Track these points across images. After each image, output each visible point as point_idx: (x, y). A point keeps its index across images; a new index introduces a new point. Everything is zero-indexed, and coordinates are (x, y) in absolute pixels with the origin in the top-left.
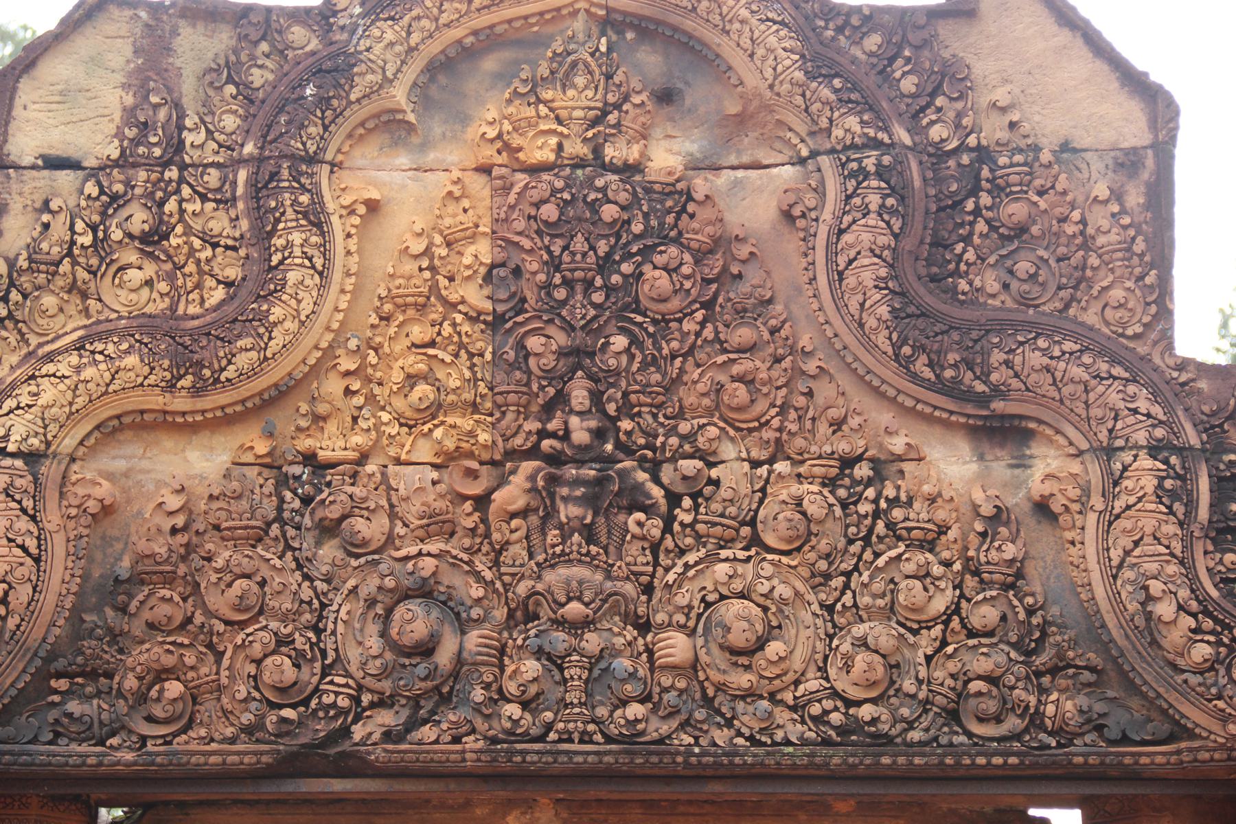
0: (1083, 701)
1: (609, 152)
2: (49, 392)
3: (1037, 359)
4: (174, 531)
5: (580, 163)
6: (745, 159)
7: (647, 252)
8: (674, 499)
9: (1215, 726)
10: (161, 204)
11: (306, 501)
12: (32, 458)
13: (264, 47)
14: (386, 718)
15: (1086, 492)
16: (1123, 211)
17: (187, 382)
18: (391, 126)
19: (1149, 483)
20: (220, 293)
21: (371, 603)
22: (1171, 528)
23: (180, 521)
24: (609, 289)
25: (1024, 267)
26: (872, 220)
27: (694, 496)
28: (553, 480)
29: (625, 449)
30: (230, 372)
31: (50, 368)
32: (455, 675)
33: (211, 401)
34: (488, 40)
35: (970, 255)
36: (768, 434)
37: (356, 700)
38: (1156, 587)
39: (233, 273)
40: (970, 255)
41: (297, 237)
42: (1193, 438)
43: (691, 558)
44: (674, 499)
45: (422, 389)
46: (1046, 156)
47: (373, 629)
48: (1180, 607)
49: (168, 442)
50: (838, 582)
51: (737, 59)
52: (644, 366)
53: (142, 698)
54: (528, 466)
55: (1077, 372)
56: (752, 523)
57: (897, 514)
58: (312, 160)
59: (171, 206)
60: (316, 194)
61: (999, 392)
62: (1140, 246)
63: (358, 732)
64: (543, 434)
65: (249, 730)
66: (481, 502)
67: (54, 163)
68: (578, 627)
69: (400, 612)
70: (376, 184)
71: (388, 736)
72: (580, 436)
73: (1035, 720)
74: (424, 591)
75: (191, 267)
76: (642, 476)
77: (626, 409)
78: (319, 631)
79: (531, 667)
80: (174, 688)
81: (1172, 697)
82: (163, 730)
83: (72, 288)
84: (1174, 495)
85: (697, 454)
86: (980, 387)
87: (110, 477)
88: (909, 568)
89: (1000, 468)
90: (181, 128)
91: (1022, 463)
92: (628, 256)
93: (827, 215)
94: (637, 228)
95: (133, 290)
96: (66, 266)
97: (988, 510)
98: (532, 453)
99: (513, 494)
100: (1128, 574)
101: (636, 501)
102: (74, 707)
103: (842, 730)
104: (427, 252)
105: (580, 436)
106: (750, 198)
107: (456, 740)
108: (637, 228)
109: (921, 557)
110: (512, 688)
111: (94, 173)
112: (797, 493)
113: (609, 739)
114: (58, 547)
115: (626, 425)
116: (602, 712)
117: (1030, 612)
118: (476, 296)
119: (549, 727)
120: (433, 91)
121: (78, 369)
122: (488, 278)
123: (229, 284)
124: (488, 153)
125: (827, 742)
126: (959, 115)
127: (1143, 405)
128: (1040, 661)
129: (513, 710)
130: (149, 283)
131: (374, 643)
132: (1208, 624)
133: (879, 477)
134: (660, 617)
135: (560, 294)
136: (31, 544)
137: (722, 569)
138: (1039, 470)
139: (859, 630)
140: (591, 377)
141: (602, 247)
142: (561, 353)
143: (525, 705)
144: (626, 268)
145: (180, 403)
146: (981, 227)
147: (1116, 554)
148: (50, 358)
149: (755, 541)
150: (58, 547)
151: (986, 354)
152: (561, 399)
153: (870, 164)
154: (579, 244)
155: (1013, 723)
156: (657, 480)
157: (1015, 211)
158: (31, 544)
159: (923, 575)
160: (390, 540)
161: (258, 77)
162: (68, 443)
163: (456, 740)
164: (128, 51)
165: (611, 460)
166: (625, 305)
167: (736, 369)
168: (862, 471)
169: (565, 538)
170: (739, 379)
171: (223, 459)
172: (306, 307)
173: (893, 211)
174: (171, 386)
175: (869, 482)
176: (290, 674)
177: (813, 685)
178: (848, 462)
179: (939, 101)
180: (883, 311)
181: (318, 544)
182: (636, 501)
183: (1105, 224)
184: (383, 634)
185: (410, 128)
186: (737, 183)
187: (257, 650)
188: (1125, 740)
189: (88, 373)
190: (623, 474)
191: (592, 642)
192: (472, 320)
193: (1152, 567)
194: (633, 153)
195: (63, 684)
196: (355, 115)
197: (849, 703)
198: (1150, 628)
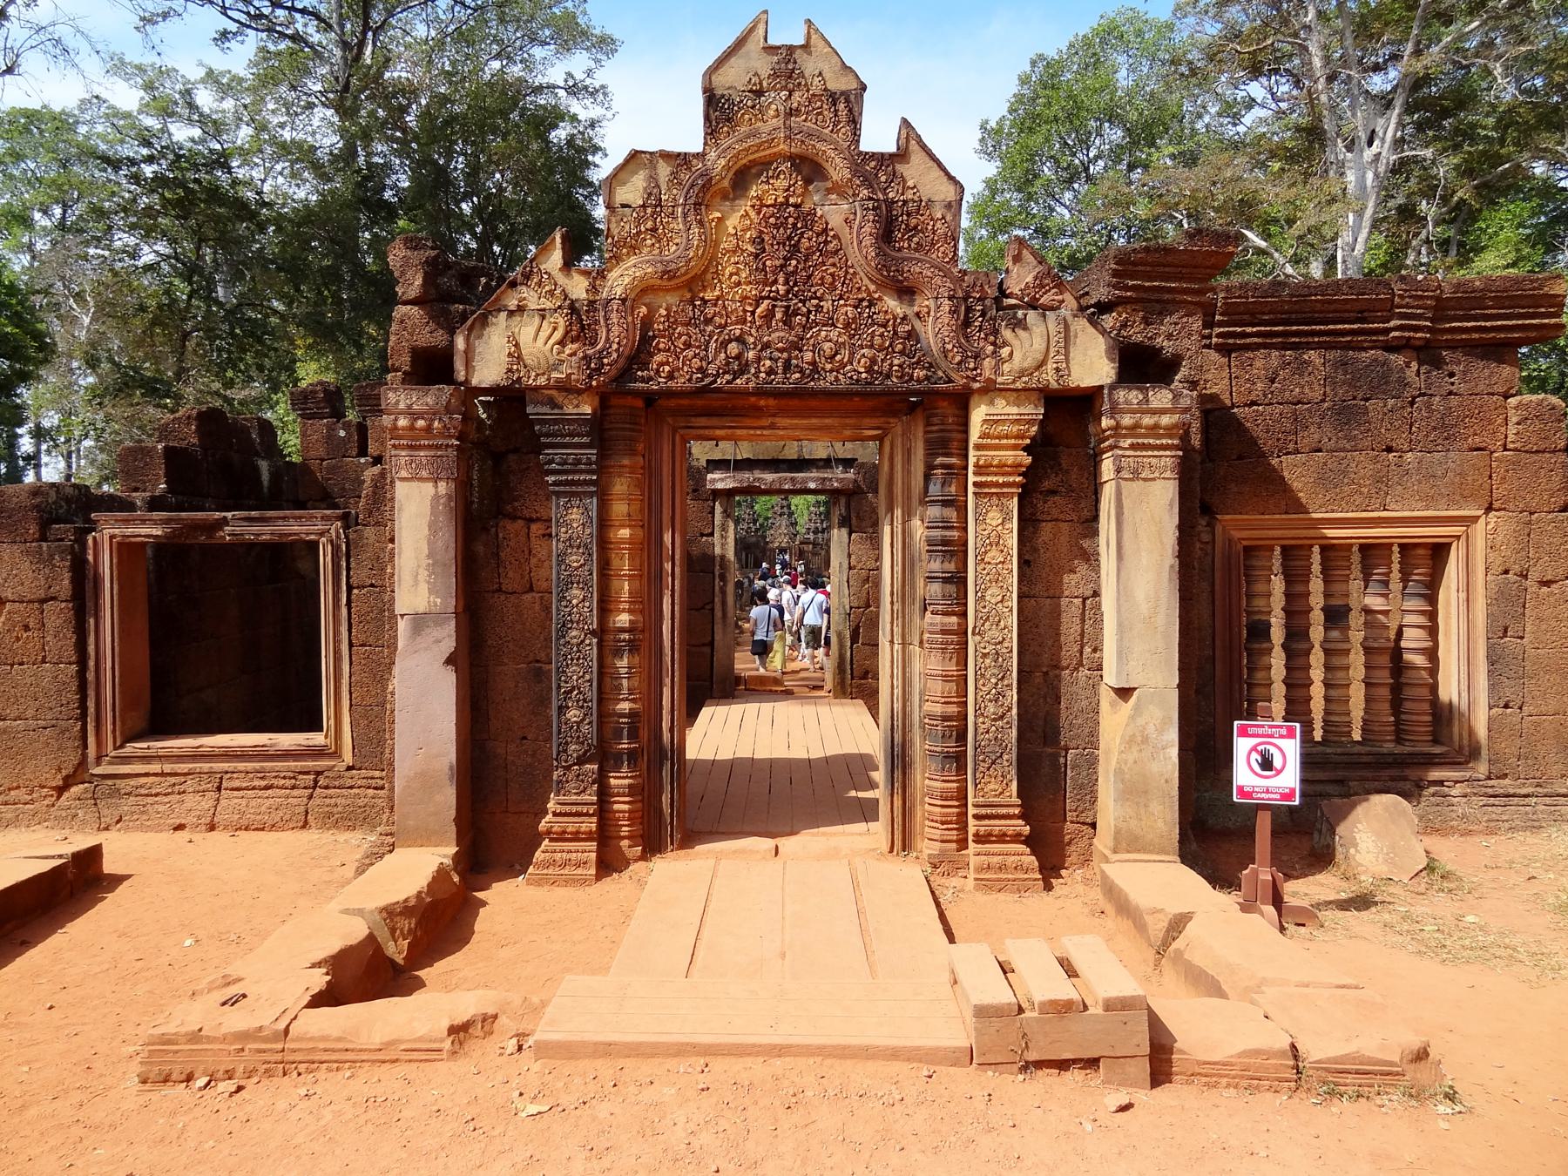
1: (792, 200)
5: (782, 204)
12: (624, 301)
14: (727, 377)
34: (754, 163)
44: (809, 312)
51: (831, 170)
65: (690, 380)
66: (753, 313)
67: (624, 206)
77: (795, 284)
79: (768, 363)
80: (667, 368)
98: (768, 298)
106: (834, 213)
129: (763, 375)
133: (871, 304)
157: (913, 222)
159: (882, 335)
178: (862, 300)
191: (785, 355)
198: (945, 352)
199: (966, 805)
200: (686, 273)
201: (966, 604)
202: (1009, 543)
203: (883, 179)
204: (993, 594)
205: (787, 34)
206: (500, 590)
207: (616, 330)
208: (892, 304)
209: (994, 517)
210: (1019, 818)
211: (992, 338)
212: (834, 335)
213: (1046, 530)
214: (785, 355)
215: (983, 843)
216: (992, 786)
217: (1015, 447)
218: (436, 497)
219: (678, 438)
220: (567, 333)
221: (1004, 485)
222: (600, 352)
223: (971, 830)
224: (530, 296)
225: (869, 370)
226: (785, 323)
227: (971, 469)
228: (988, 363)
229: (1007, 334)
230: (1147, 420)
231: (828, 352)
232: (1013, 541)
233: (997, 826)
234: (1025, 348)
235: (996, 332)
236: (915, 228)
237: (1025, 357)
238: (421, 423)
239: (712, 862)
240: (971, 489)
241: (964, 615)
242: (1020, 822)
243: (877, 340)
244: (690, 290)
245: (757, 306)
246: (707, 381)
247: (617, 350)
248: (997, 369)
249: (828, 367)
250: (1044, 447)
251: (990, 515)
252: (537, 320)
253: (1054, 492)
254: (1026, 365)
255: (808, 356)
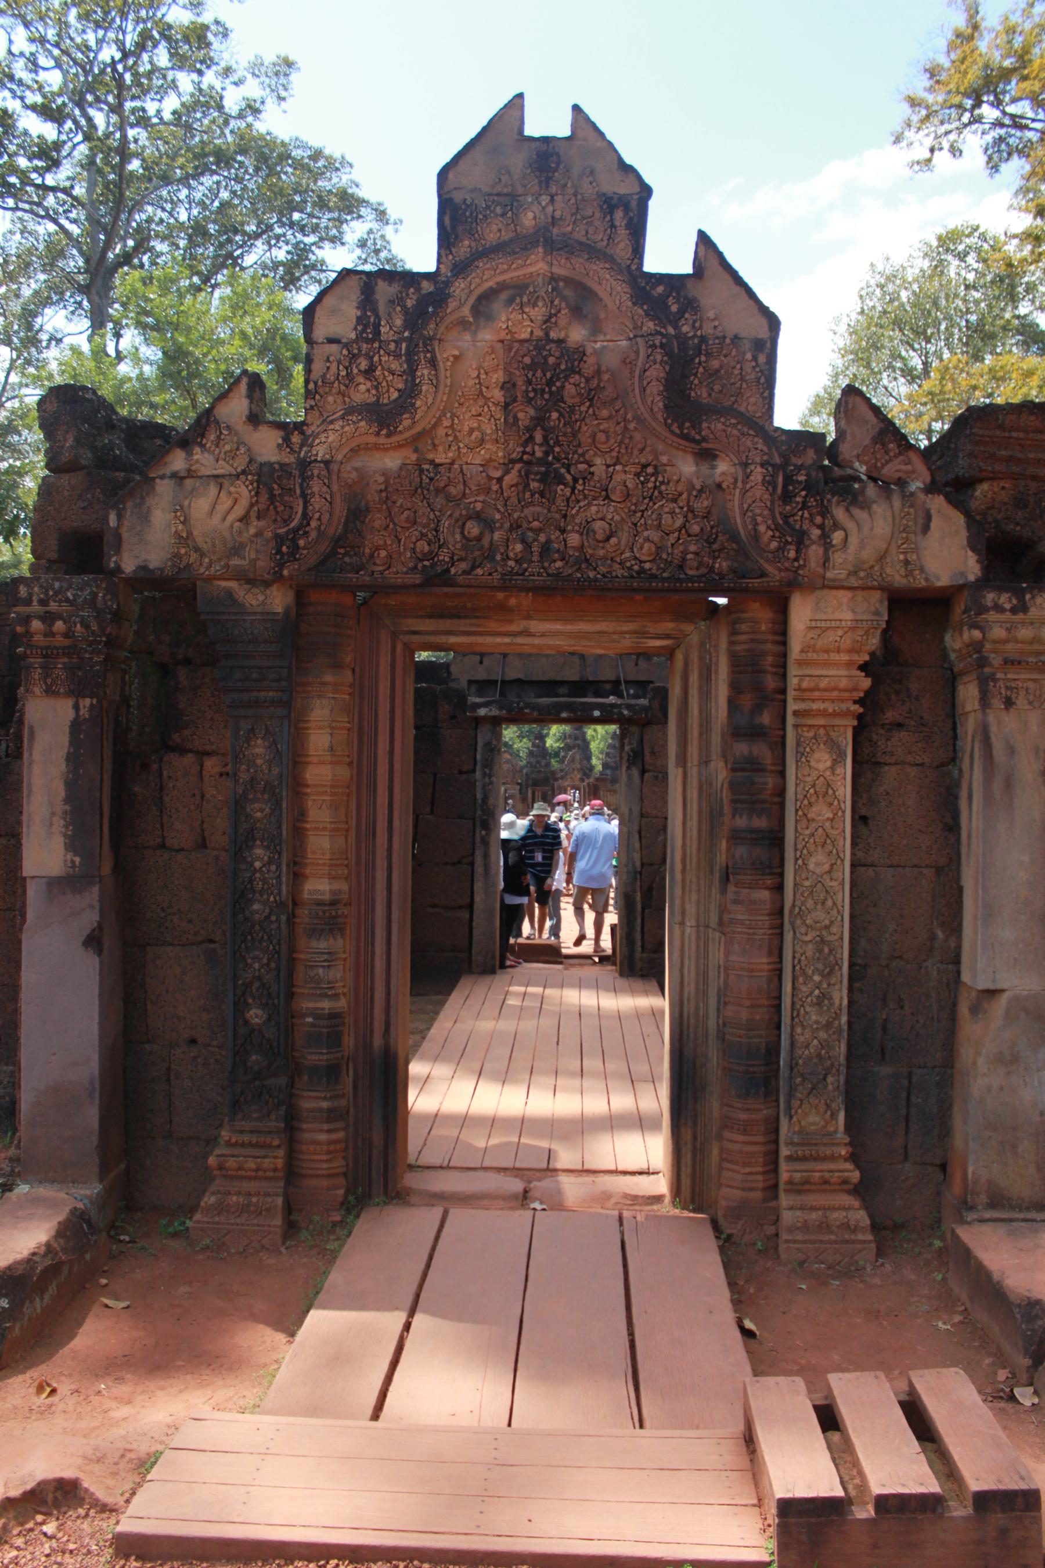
0: (729, 563)
2: (332, 437)
3: (720, 426)
4: (381, 491)
6: (608, 337)
7: (566, 378)
8: (575, 480)
9: (776, 573)
10: (372, 358)
11: (431, 479)
12: (327, 463)
13: (412, 290)
14: (464, 566)
15: (736, 480)
16: (757, 365)
17: (384, 432)
18: (463, 324)
19: (760, 478)
20: (396, 395)
21: (457, 520)
22: (767, 496)
23: (383, 487)
24: (551, 393)
25: (717, 388)
26: (657, 366)
27: (584, 479)
28: (527, 473)
29: (557, 459)
30: (401, 428)
31: (332, 427)
32: (490, 549)
33: (394, 439)
34: (502, 287)
35: (696, 382)
36: (614, 454)
37: (452, 558)
38: (759, 519)
39: (401, 386)
40: (696, 382)
41: (426, 372)
42: (777, 460)
43: (582, 504)
44: (575, 480)
45: (476, 434)
46: (728, 341)
47: (458, 530)
48: (768, 527)
49: (377, 455)
50: (639, 514)
52: (565, 425)
53: (372, 556)
54: (518, 466)
55: (735, 432)
56: (606, 490)
57: (663, 488)
58: (431, 339)
59: (376, 359)
60: (433, 352)
61: (704, 439)
62: (762, 380)
63: (453, 571)
64: (524, 453)
66: (500, 480)
67: (331, 341)
68: (537, 531)
69: (469, 524)
70: (458, 348)
71: (464, 572)
72: (539, 454)
73: (711, 569)
74: (478, 516)
75: (384, 384)
76: (563, 471)
77: (557, 443)
78: (437, 531)
79: (519, 547)
81: (762, 562)
82: (381, 568)
83: (339, 393)
84: (769, 483)
85: (586, 462)
86: (697, 437)
87: (356, 469)
88: (666, 510)
89: (705, 469)
90: (379, 325)
91: (713, 467)
92: (559, 379)
93: (639, 363)
94: (563, 367)
95: (362, 393)
96: (336, 384)
97: (698, 487)
98: (520, 460)
99: (511, 479)
100: (750, 514)
101: (560, 480)
102: (347, 560)
103: (638, 573)
104: (478, 377)
105: (539, 454)
107: (490, 574)
108: (563, 367)
109: (672, 505)
110: (511, 555)
111: (346, 346)
112: (624, 477)
113: (549, 575)
114: (338, 498)
115: (557, 449)
116: (546, 564)
117: (712, 527)
118: (498, 395)
119: (526, 570)
120: (481, 308)
121: (343, 427)
122: (502, 388)
123: (399, 391)
124: (503, 335)
125: (632, 577)
126: (694, 322)
127: (760, 446)
128: (715, 546)
129: (511, 563)
130: (368, 390)
131: (458, 537)
132: (777, 534)
134: (569, 528)
135: (531, 395)
136: (328, 497)
137: (594, 509)
138: (719, 471)
139: (646, 534)
140: (543, 429)
141: (548, 375)
142: (532, 419)
143: (516, 561)
144: (558, 384)
145: (382, 440)
146: (701, 370)
147: (745, 506)
148: (332, 422)
149: (607, 497)
150: (338, 498)
151: (700, 423)
152: (531, 439)
153: (657, 342)
154: (539, 374)
155: (703, 570)
156: (569, 472)
157: (715, 364)
158: (328, 497)
159: (672, 513)
160: (464, 494)
161: (409, 303)
162: (339, 457)
163: (490, 574)
164: (358, 293)
165: (551, 464)
166: (557, 398)
167: (601, 427)
168: (650, 470)
169: (532, 495)
170: (603, 431)
171: (399, 462)
172: (430, 401)
173: (666, 363)
174: (378, 434)
175: (653, 475)
176: (427, 548)
177: (627, 555)
178: (645, 466)
179: (687, 315)
180: (661, 404)
181: (437, 496)
182: (560, 480)
183: (749, 370)
184: (462, 533)
185: (471, 323)
186: (604, 347)
187: (414, 539)
188: (744, 577)
189: (347, 429)
190: (556, 470)
192: (496, 405)
193: (758, 511)
194: (562, 335)
195: (342, 551)
196: (448, 320)
197: (641, 562)
198: (756, 536)
199: (776, 1142)
200: (409, 428)
201: (781, 875)
202: (840, 793)
203: (674, 308)
204: (818, 862)
205: (548, 120)
206: (163, 846)
207: (317, 503)
208: (687, 467)
209: (822, 760)
210: (846, 1160)
211: (818, 520)
212: (609, 512)
213: (890, 775)
214: (542, 538)
215: (799, 1192)
216: (812, 1118)
217: (849, 665)
218: (75, 726)
219: (399, 647)
220: (252, 505)
221: (834, 715)
222: (295, 531)
223: (784, 1176)
224: (204, 461)
225: (656, 558)
226: (542, 494)
227: (791, 694)
228: (814, 552)
229: (839, 513)
230: (1025, 633)
231: (600, 536)
232: (845, 791)
233: (818, 1170)
234: (866, 533)
235: (825, 512)
236: (718, 371)
237: (862, 545)
238: (59, 625)
239: (437, 1213)
240: (790, 720)
241: (779, 888)
242: (849, 1166)
243: (666, 519)
244: (416, 450)
245: (507, 472)
246: (439, 569)
247: (318, 528)
248: (826, 560)
249: (602, 553)
250: (884, 667)
251: (817, 755)
252: (213, 490)
253: (900, 726)
254: (865, 554)
255: (574, 539)
